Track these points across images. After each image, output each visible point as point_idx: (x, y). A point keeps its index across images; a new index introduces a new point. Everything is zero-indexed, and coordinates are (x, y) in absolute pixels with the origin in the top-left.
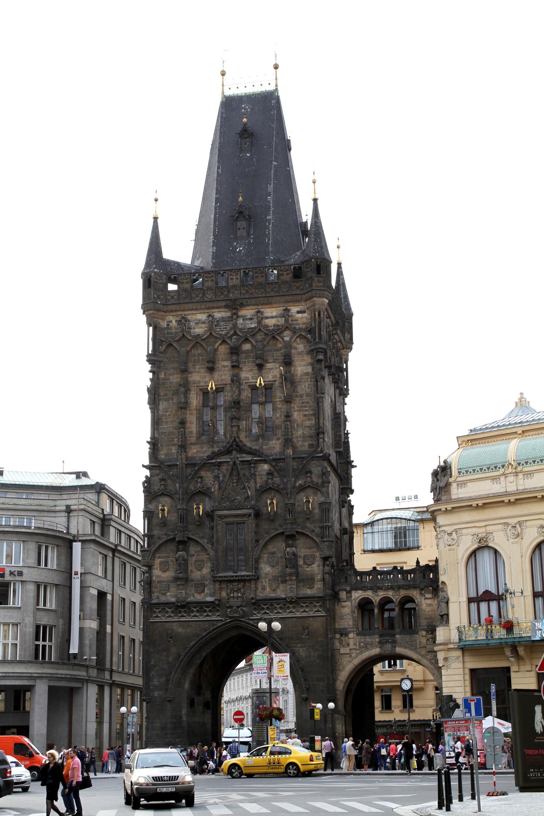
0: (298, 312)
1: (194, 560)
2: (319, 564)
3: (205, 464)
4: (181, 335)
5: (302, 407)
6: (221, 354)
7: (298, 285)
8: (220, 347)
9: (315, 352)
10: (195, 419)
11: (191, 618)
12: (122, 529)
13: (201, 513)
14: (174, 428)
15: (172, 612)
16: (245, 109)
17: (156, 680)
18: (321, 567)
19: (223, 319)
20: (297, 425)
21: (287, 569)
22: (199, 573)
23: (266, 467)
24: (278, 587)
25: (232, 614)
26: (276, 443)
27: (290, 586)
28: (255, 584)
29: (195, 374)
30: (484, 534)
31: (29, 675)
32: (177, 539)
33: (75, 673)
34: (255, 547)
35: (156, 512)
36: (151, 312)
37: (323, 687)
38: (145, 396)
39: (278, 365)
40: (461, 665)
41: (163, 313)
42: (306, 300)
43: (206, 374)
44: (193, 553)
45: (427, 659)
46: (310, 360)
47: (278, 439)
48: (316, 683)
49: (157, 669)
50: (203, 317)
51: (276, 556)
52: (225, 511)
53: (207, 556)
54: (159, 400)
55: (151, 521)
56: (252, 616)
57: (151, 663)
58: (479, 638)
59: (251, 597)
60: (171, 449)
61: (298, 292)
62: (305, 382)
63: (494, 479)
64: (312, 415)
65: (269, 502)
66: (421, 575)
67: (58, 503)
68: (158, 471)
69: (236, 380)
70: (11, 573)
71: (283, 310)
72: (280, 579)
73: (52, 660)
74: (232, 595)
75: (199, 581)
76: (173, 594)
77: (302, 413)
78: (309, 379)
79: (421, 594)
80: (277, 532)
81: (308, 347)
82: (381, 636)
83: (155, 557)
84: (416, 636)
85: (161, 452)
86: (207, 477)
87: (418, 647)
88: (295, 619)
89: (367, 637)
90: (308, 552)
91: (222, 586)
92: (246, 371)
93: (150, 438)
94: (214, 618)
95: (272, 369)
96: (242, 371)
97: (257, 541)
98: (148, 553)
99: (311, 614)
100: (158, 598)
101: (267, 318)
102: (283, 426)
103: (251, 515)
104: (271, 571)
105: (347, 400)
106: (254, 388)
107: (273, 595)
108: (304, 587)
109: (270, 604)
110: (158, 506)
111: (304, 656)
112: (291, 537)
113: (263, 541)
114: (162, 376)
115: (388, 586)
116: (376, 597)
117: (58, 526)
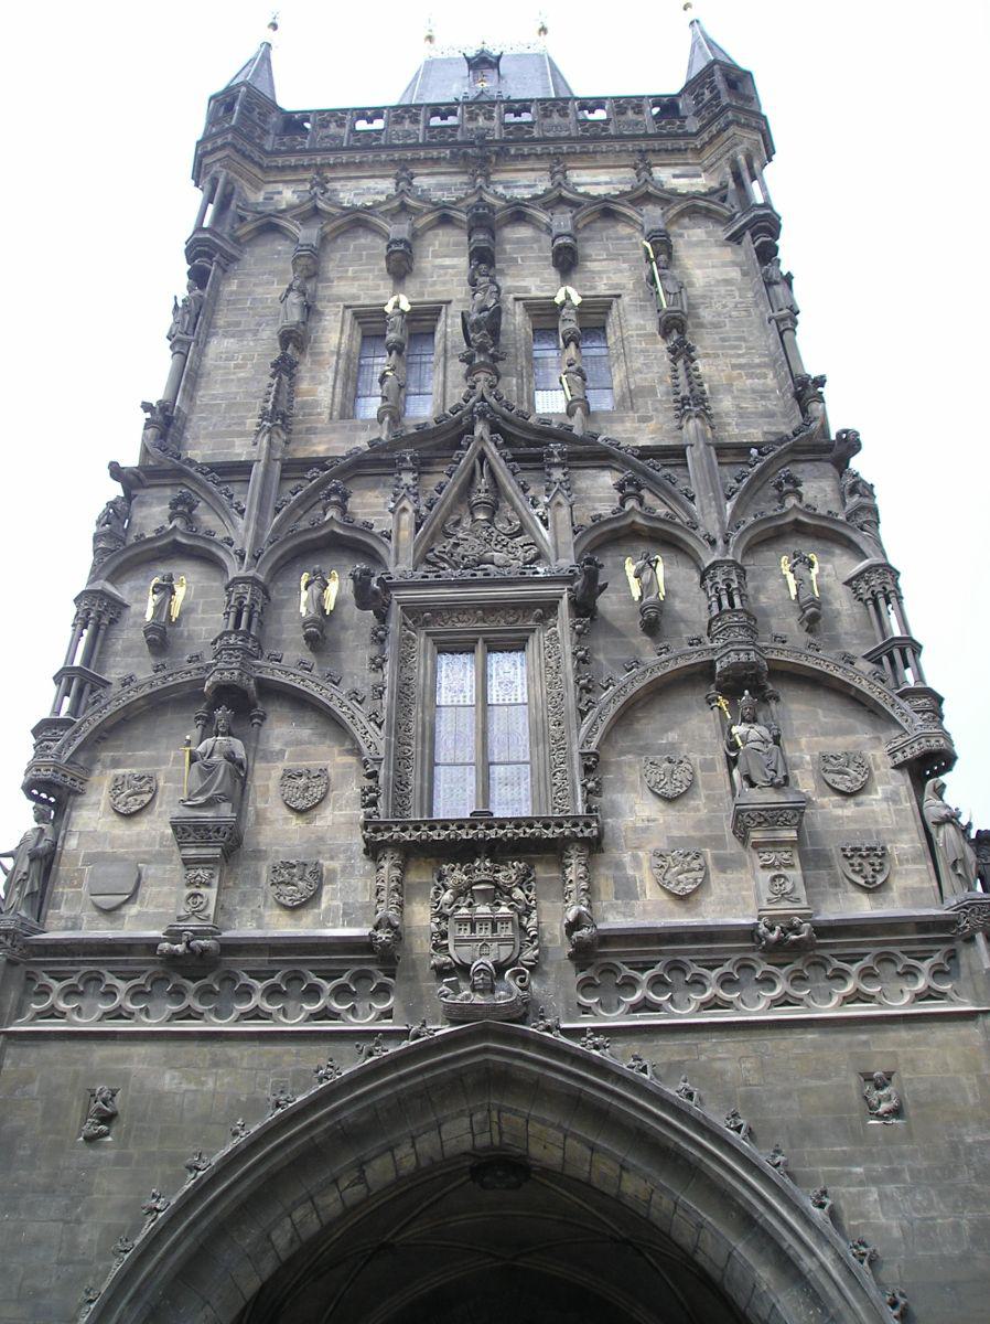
0: (675, 176)
1: (277, 773)
2: (896, 792)
4: (308, 206)
5: (723, 348)
9: (748, 234)
14: (247, 394)
18: (908, 805)
22: (295, 823)
24: (702, 887)
25: (467, 997)
27: (776, 873)
28: (589, 866)
29: (342, 283)
34: (583, 714)
35: (135, 608)
36: (219, 155)
38: (166, 321)
41: (256, 171)
42: (703, 147)
43: (382, 283)
44: (277, 746)
51: (681, 758)
53: (352, 760)
54: (208, 336)
55: (106, 638)
59: (571, 915)
72: (708, 852)
74: (464, 911)
76: (151, 910)
78: (737, 294)
80: (682, 663)
83: (93, 761)
88: (811, 1036)
91: (413, 877)
93: (159, 402)
96: (502, 272)
98: (67, 733)
99: (901, 1005)
101: (579, 185)
102: (660, 389)
103: (550, 608)
109: (666, 959)
111: (897, 1233)
113: (617, 695)
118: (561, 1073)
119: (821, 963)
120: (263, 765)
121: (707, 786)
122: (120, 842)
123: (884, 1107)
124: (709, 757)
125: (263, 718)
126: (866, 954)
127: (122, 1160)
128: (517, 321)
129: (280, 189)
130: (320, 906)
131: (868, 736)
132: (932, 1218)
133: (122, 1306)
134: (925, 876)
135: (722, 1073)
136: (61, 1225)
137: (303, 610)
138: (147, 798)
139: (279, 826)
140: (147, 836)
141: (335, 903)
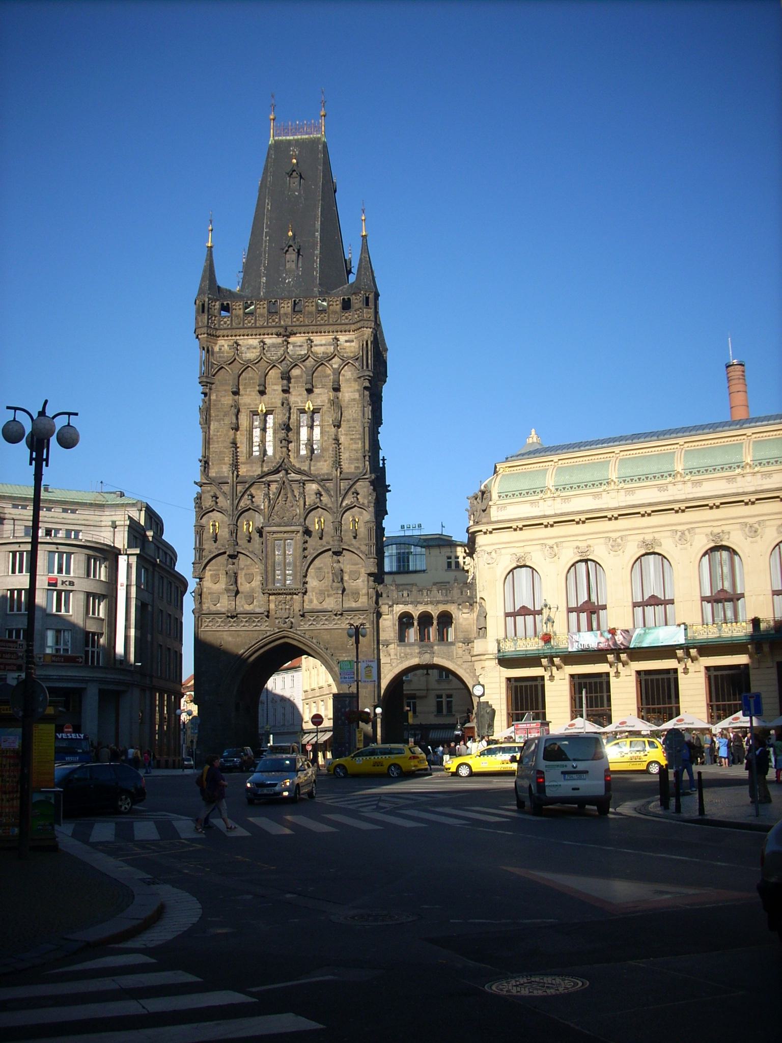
0: (346, 341)
1: (243, 573)
3: (254, 482)
6: (271, 378)
7: (346, 315)
8: (270, 372)
10: (245, 440)
12: (160, 546)
13: (251, 530)
14: (225, 447)
16: (293, 151)
18: (366, 583)
19: (274, 345)
20: (344, 448)
22: (248, 585)
23: (313, 487)
26: (323, 465)
30: (523, 554)
31: (81, 678)
32: (228, 553)
33: (121, 677)
35: (207, 527)
39: (326, 391)
40: (497, 674)
43: (257, 397)
44: (243, 567)
45: (462, 668)
46: (357, 387)
47: (326, 461)
50: (254, 342)
58: (517, 649)
60: (222, 467)
61: (347, 321)
62: (352, 407)
63: (532, 503)
64: (359, 439)
65: (316, 520)
66: (459, 591)
67: (103, 518)
68: (209, 488)
69: (285, 404)
70: (63, 583)
71: (333, 339)
72: (326, 593)
73: (101, 665)
75: (248, 593)
77: (349, 437)
78: (356, 405)
79: (459, 608)
80: (325, 549)
81: (355, 375)
84: (452, 647)
85: (213, 470)
86: (257, 495)
87: (455, 657)
88: (340, 631)
89: (407, 648)
90: (354, 568)
92: (295, 395)
94: (263, 628)
95: (321, 394)
96: (292, 395)
97: (305, 557)
100: (209, 608)
101: (316, 345)
105: (380, 429)
106: (303, 411)
107: (319, 607)
110: (208, 522)
112: (337, 553)
114: (213, 397)
115: (428, 601)
116: (416, 611)
117: (105, 540)
118: (297, 637)
128: (294, 417)
129: (223, 344)
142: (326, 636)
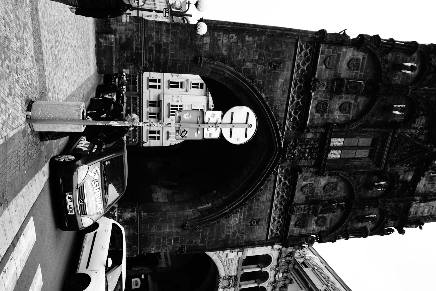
2: (315, 231)
11: (292, 95)
15: (303, 71)
17: (225, 41)
21: (321, 207)
22: (337, 106)
24: (304, 193)
27: (303, 208)
37: (194, 242)
44: (358, 101)
47: (424, 185)
48: (201, 236)
49: (239, 44)
52: (390, 141)
56: (280, 167)
57: (247, 36)
64: (431, 213)
82: (236, 277)
88: (268, 211)
98: (375, 47)
99: (271, 227)
102: (432, 190)
104: (321, 185)
108: (298, 218)
113: (352, 180)
119: (282, 214)
120: (354, 97)
121: (325, 195)
122: (342, 62)
123: (253, 223)
124: (332, 196)
125: (367, 97)
126: (283, 222)
127: (265, 71)
130: (316, 113)
131: (328, 227)
132: (231, 228)
133: (234, 76)
134: (296, 234)
135: (264, 195)
136: (252, 59)
137: (395, 106)
138: (352, 69)
139: (338, 102)
140: (342, 69)
141: (316, 117)
142: (266, 197)
